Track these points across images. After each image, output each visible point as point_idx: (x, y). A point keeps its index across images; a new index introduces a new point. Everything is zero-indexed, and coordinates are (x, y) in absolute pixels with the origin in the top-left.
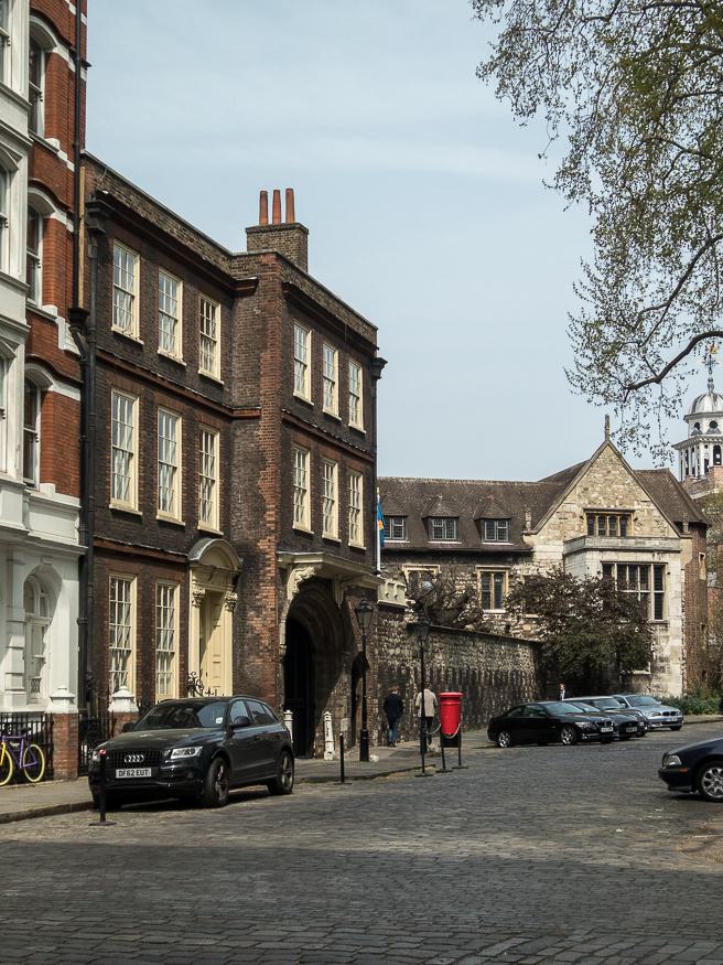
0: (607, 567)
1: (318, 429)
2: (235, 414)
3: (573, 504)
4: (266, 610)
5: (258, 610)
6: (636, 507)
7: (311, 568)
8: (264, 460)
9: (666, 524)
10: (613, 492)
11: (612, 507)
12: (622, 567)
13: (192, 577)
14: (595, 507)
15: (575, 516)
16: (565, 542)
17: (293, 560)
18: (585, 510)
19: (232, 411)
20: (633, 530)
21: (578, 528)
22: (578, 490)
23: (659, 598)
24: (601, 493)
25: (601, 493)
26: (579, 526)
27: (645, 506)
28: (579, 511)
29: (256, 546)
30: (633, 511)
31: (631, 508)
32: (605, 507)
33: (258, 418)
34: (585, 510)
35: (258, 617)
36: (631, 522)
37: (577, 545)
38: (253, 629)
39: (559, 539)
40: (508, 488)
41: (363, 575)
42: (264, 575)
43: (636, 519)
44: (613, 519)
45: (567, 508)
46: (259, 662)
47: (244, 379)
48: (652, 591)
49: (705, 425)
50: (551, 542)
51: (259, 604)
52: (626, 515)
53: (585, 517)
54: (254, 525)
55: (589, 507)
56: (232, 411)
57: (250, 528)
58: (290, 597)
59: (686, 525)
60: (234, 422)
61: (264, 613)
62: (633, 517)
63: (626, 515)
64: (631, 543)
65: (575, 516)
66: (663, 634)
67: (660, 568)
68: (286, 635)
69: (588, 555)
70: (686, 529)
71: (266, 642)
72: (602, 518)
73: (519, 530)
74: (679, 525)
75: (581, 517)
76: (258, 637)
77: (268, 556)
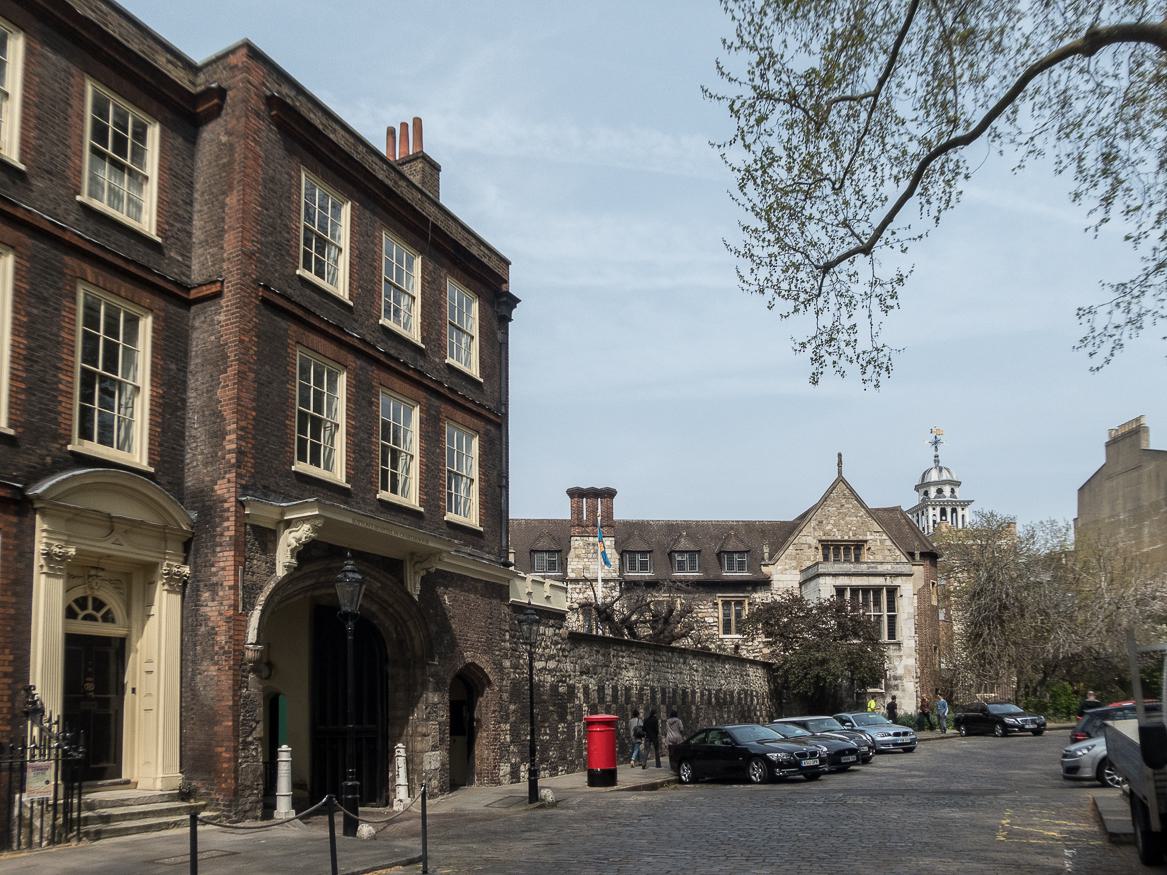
0: (840, 591)
2: (193, 294)
3: (809, 537)
4: (223, 589)
5: (213, 588)
6: (869, 537)
7: (306, 527)
8: (225, 357)
9: (898, 553)
10: (847, 524)
11: (846, 538)
12: (855, 590)
13: (40, 524)
14: (829, 538)
15: (810, 547)
16: (801, 571)
17: (283, 514)
18: (820, 541)
19: (188, 290)
20: (866, 557)
21: (814, 555)
22: (813, 523)
23: (892, 620)
24: (834, 525)
25: (834, 525)
26: (815, 556)
27: (877, 536)
28: (814, 542)
29: (213, 490)
30: (866, 541)
31: (865, 538)
32: (839, 538)
33: (218, 295)
34: (820, 541)
35: (213, 600)
36: (864, 550)
37: (812, 572)
38: (207, 619)
39: (795, 568)
40: (749, 527)
41: (440, 552)
42: (222, 535)
43: (869, 548)
44: (847, 548)
45: (803, 540)
46: (213, 670)
47: (205, 243)
48: (885, 613)
49: (933, 492)
50: (787, 572)
51: (214, 579)
52: (859, 545)
53: (820, 547)
54: (213, 459)
55: (824, 538)
56: (188, 290)
57: (206, 465)
58: (281, 572)
59: (917, 553)
60: (193, 309)
61: (221, 593)
62: (866, 548)
63: (859, 545)
64: (863, 568)
65: (810, 547)
66: (897, 653)
67: (892, 591)
68: (259, 629)
69: (822, 580)
70: (917, 557)
71: (222, 639)
72: (837, 548)
73: (757, 561)
74: (912, 555)
75: (817, 548)
76: (212, 633)
77: (226, 505)
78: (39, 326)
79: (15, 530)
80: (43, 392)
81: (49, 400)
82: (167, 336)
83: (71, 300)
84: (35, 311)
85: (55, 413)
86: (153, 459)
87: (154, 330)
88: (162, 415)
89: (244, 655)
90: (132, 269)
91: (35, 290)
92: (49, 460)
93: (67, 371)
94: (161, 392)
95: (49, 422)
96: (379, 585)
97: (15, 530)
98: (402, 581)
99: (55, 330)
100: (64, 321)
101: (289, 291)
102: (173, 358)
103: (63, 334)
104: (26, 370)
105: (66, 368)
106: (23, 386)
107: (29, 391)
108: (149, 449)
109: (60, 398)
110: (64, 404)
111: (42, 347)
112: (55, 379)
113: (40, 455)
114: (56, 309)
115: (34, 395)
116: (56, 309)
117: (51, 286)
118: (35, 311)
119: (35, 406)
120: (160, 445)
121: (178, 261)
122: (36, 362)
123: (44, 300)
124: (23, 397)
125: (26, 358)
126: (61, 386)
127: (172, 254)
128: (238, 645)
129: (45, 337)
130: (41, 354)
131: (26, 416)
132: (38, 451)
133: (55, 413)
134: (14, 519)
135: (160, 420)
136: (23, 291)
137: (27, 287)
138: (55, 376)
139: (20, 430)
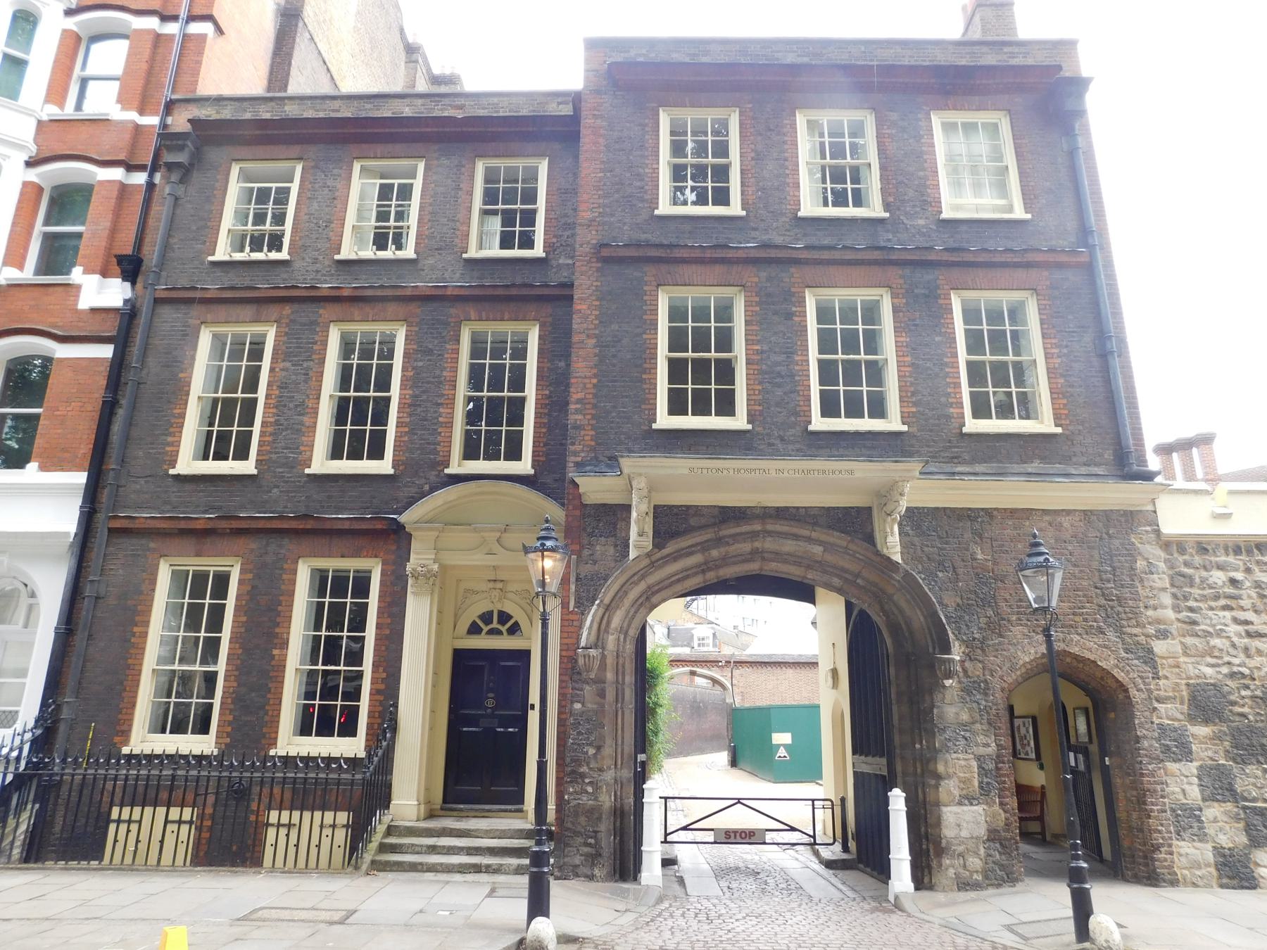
1: (765, 246)
78: (424, 375)
79: (393, 557)
80: (424, 430)
81: (430, 434)
82: (554, 338)
83: (454, 342)
84: (420, 364)
85: (434, 444)
86: (538, 461)
87: (540, 337)
88: (549, 415)
89: (576, 661)
90: (514, 292)
91: (421, 346)
92: (427, 487)
93: (447, 404)
94: (547, 392)
95: (430, 453)
96: (821, 549)
97: (393, 557)
98: (870, 539)
99: (438, 372)
100: (447, 362)
101: (643, 237)
102: (562, 355)
103: (445, 374)
104: (410, 415)
105: (447, 402)
106: (407, 429)
107: (412, 432)
108: (533, 452)
109: (439, 430)
110: (443, 434)
111: (424, 392)
112: (436, 415)
113: (418, 485)
114: (439, 355)
115: (416, 434)
116: (439, 355)
117: (437, 338)
118: (420, 364)
119: (416, 444)
120: (545, 445)
121: (568, 265)
122: (420, 406)
123: (429, 352)
124: (406, 439)
125: (410, 406)
126: (441, 419)
127: (561, 261)
128: (567, 650)
129: (428, 383)
130: (424, 397)
131: (407, 455)
132: (417, 482)
133: (434, 444)
134: (394, 548)
135: (546, 421)
136: (411, 351)
137: (415, 347)
138: (436, 412)
139: (401, 468)
